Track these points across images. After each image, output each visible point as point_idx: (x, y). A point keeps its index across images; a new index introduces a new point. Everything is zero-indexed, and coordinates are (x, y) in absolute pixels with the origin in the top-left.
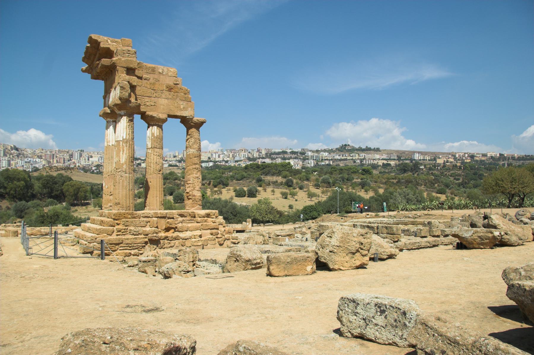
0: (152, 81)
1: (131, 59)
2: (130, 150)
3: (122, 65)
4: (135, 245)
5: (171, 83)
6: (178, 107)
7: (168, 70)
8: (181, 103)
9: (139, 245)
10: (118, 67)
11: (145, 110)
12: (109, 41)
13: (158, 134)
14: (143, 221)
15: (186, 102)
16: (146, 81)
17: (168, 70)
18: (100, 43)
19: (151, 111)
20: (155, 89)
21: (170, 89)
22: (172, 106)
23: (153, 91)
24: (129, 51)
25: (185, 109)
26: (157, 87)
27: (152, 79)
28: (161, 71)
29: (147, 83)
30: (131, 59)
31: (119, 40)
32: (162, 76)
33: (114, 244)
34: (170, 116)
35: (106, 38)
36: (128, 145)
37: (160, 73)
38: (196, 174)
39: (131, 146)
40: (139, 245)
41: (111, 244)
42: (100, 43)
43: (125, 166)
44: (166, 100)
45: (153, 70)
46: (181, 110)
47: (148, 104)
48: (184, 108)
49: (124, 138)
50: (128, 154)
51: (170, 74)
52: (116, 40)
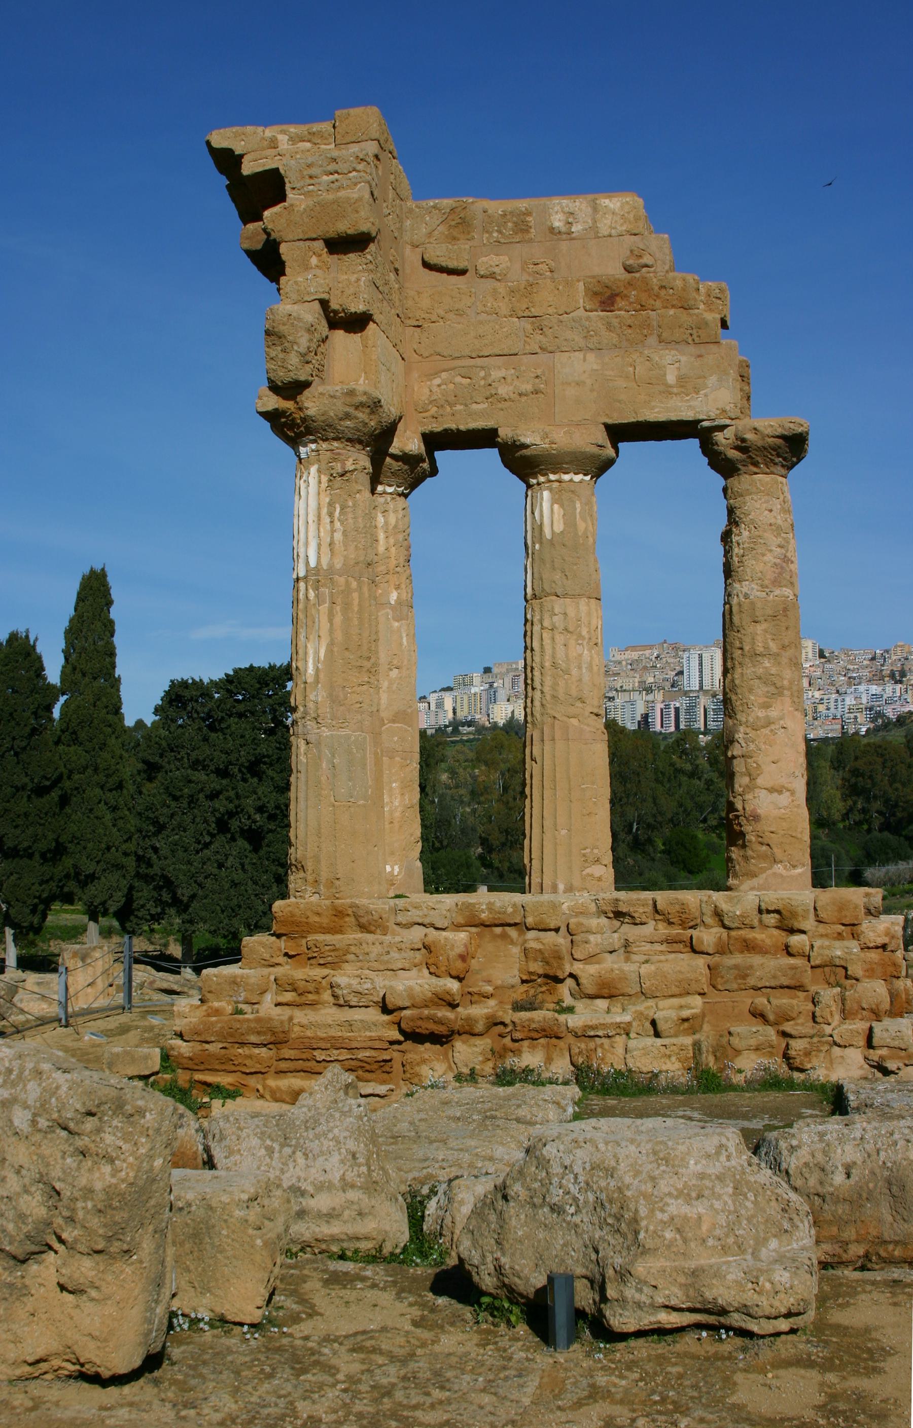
5: (613, 270)
10: (283, 249)
12: (283, 139)
13: (559, 527)
15: (692, 349)
16: (489, 284)
18: (241, 156)
20: (534, 311)
21: (606, 298)
23: (527, 325)
28: (558, 222)
30: (342, 194)
31: (326, 126)
32: (564, 246)
34: (619, 433)
35: (269, 132)
42: (241, 156)
44: (591, 357)
46: (667, 391)
47: (503, 391)
49: (313, 564)
52: (316, 127)
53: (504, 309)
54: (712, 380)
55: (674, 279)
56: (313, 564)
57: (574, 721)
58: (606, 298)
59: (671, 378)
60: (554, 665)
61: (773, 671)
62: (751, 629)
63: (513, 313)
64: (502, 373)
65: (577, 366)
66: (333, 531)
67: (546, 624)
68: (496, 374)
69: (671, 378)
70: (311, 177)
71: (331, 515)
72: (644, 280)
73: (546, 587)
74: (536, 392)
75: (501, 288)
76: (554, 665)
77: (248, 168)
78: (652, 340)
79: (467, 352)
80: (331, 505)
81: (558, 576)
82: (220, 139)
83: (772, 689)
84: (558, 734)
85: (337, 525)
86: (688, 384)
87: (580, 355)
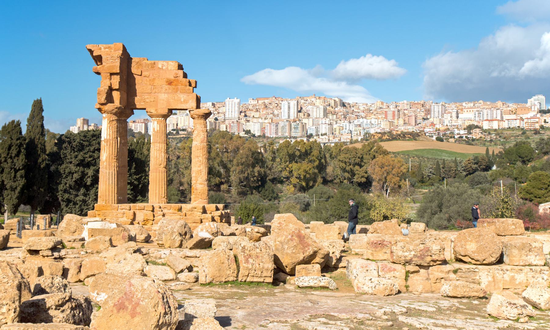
0: (151, 77)
1: (114, 64)
2: (111, 149)
5: (172, 77)
13: (158, 129)
15: (187, 94)
16: (146, 78)
21: (170, 83)
27: (151, 75)
28: (160, 66)
30: (114, 64)
32: (161, 71)
36: (108, 143)
38: (199, 167)
39: (111, 145)
43: (105, 164)
46: (181, 103)
47: (147, 100)
48: (184, 100)
50: (108, 153)
52: (109, 45)
53: (148, 84)
54: (190, 101)
58: (170, 83)
59: (182, 100)
63: (150, 85)
65: (163, 97)
68: (146, 97)
69: (182, 100)
72: (178, 80)
75: (148, 79)
77: (95, 54)
82: (89, 47)
86: (186, 102)
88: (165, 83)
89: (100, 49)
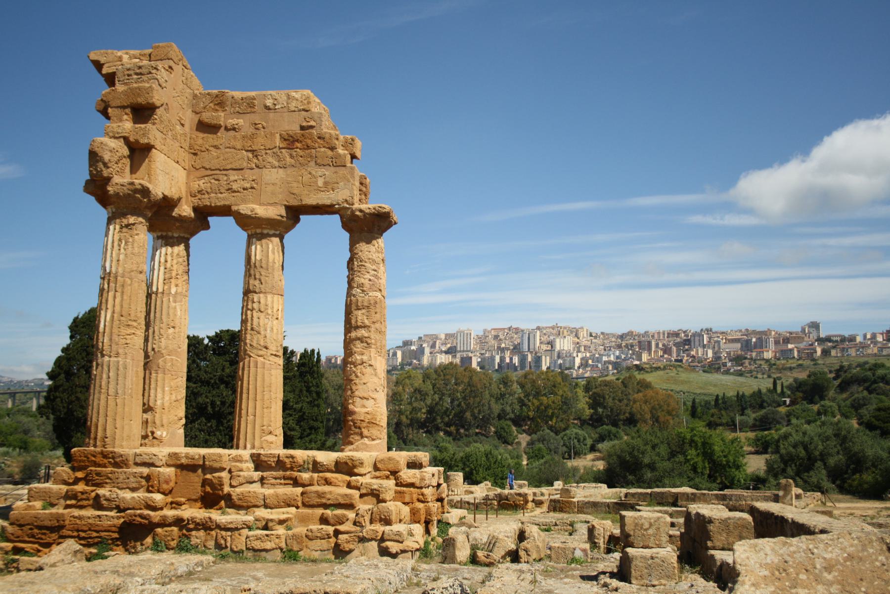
0: (248, 130)
3: (118, 103)
4: (95, 534)
6: (311, 186)
7: (288, 97)
8: (320, 173)
9: (103, 534)
11: (227, 203)
12: (125, 58)
14: (134, 475)
15: (332, 168)
16: (232, 133)
17: (288, 97)
19: (244, 201)
20: (254, 148)
21: (290, 141)
22: (295, 185)
24: (140, 67)
25: (329, 186)
26: (259, 143)
29: (235, 138)
32: (272, 115)
33: (47, 528)
35: (119, 54)
37: (267, 108)
40: (103, 534)
41: (40, 528)
44: (281, 171)
45: (250, 104)
47: (235, 186)
51: (293, 105)
55: (326, 133)
56: (108, 271)
57: (261, 359)
60: (252, 329)
61: (366, 335)
62: (355, 312)
64: (236, 177)
65: (273, 176)
66: (119, 255)
67: (250, 307)
68: (232, 178)
69: (320, 182)
70: (129, 75)
71: (119, 246)
72: (311, 134)
73: (251, 288)
74: (252, 188)
76: (252, 329)
78: (312, 164)
79: (218, 167)
80: (120, 240)
81: (257, 283)
82: (93, 56)
83: (365, 345)
84: (252, 365)
85: (122, 250)
87: (275, 170)
88: (278, 142)
89: (120, 59)
